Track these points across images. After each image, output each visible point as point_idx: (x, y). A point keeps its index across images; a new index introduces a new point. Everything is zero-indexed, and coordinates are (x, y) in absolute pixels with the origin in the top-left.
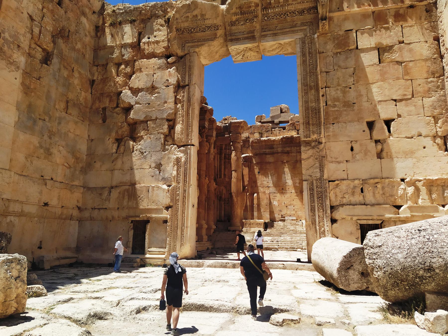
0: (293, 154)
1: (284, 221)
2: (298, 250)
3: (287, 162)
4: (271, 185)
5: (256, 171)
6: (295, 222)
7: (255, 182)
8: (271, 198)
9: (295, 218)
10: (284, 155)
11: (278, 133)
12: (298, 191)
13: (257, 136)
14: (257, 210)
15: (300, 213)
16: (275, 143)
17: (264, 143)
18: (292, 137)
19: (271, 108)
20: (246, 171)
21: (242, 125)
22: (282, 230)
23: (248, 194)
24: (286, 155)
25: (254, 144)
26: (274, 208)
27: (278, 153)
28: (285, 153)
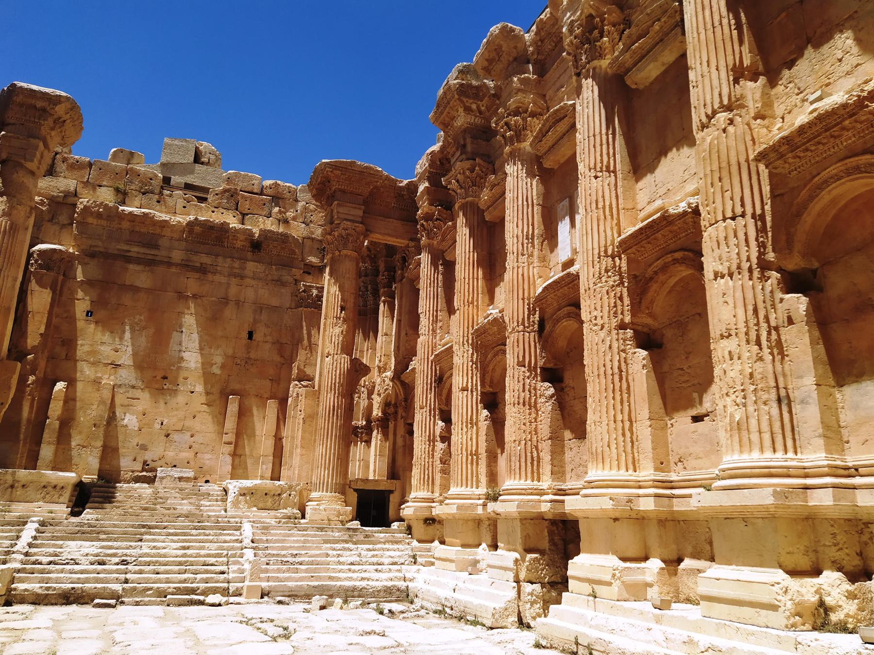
0: (218, 278)
1: (151, 481)
2: (211, 599)
3: (195, 296)
4: (126, 358)
5: (81, 306)
6: (189, 485)
7: (70, 343)
8: (118, 401)
9: (191, 474)
10: (189, 274)
11: (179, 207)
12: (216, 390)
13: (106, 196)
14: (54, 439)
15: (207, 458)
16: (167, 232)
17: (125, 225)
18: (223, 228)
19: (166, 140)
20: (40, 300)
21: (60, 110)
22: (146, 513)
23: (32, 378)
24: (197, 275)
25: (90, 220)
26: (121, 438)
27: (169, 264)
28: (195, 269)
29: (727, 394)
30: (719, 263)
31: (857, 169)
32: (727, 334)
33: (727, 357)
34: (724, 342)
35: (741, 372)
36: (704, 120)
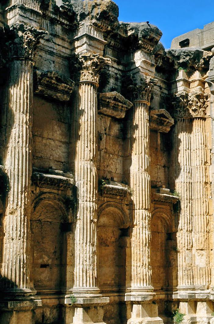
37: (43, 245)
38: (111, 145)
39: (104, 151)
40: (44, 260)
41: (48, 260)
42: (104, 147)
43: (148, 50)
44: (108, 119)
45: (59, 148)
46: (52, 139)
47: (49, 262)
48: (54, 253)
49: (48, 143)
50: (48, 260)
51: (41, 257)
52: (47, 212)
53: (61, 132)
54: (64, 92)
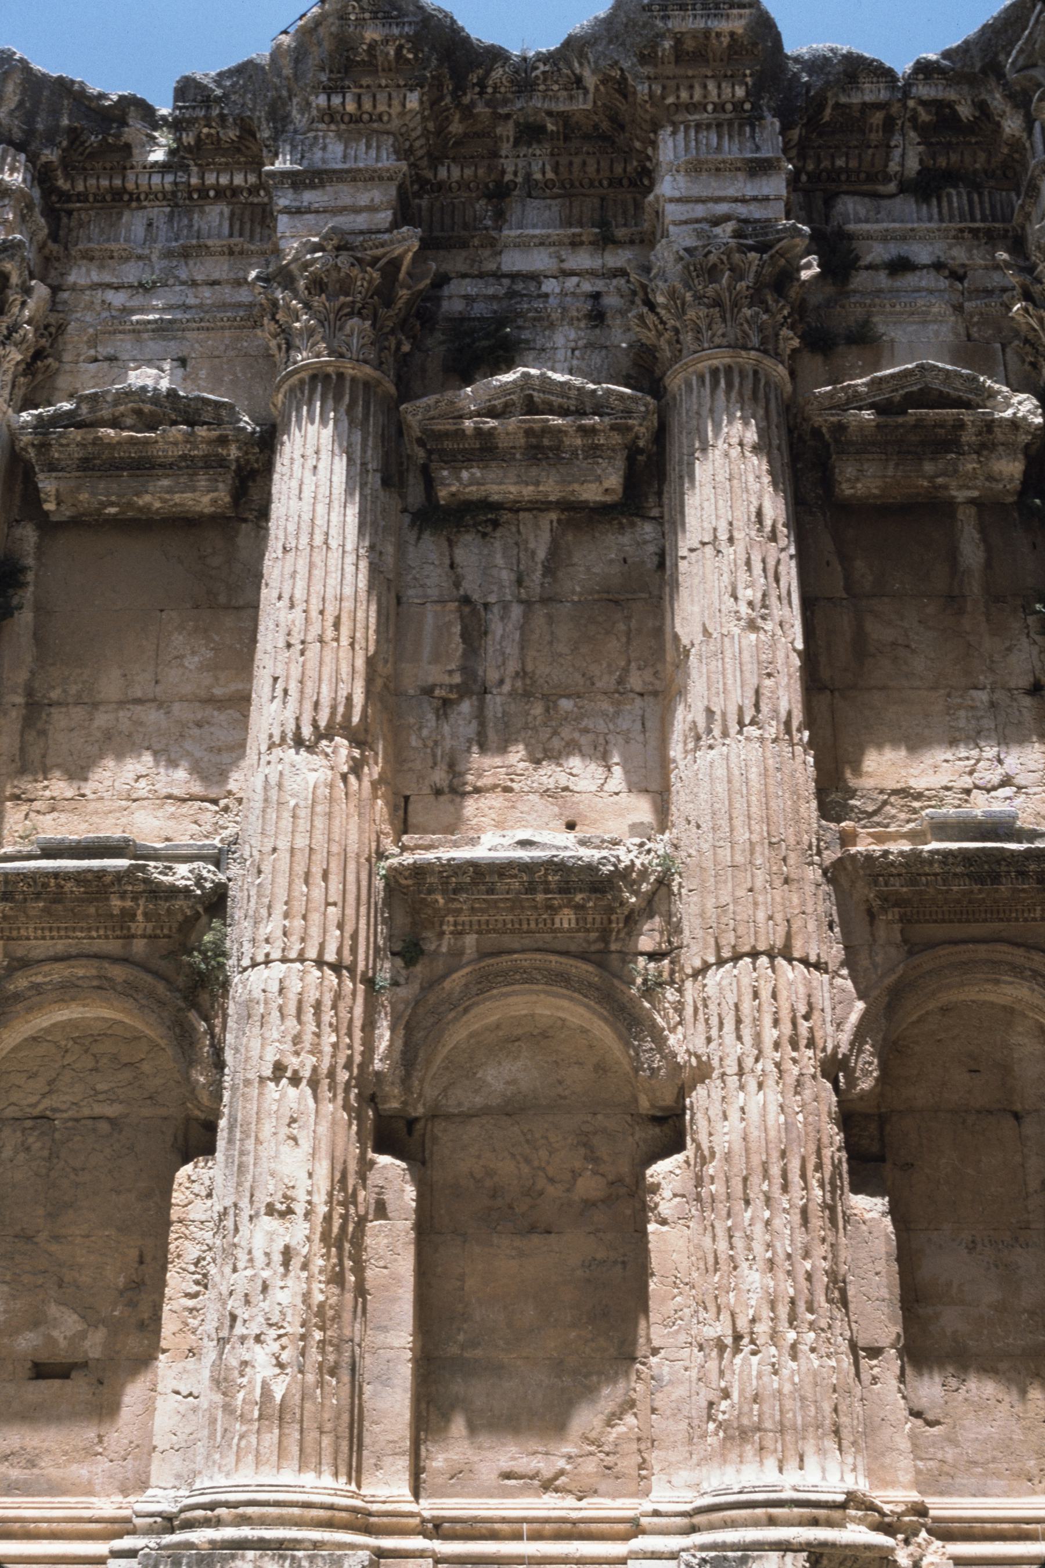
29: (258, 1339)
30: (288, 1047)
31: (562, 979)
32: (283, 1207)
33: (277, 1258)
34: (268, 1223)
35: (306, 1296)
36: (307, 732)
37: (54, 1248)
38: (562, 648)
39: (506, 688)
40: (55, 1333)
41: (83, 1335)
42: (513, 666)
43: (720, 107)
44: (537, 526)
45: (196, 731)
46: (154, 700)
47: (87, 1343)
48: (126, 1289)
49: (125, 726)
50: (83, 1335)
51: (37, 1320)
52: (95, 1070)
53: (210, 654)
54: (187, 466)
